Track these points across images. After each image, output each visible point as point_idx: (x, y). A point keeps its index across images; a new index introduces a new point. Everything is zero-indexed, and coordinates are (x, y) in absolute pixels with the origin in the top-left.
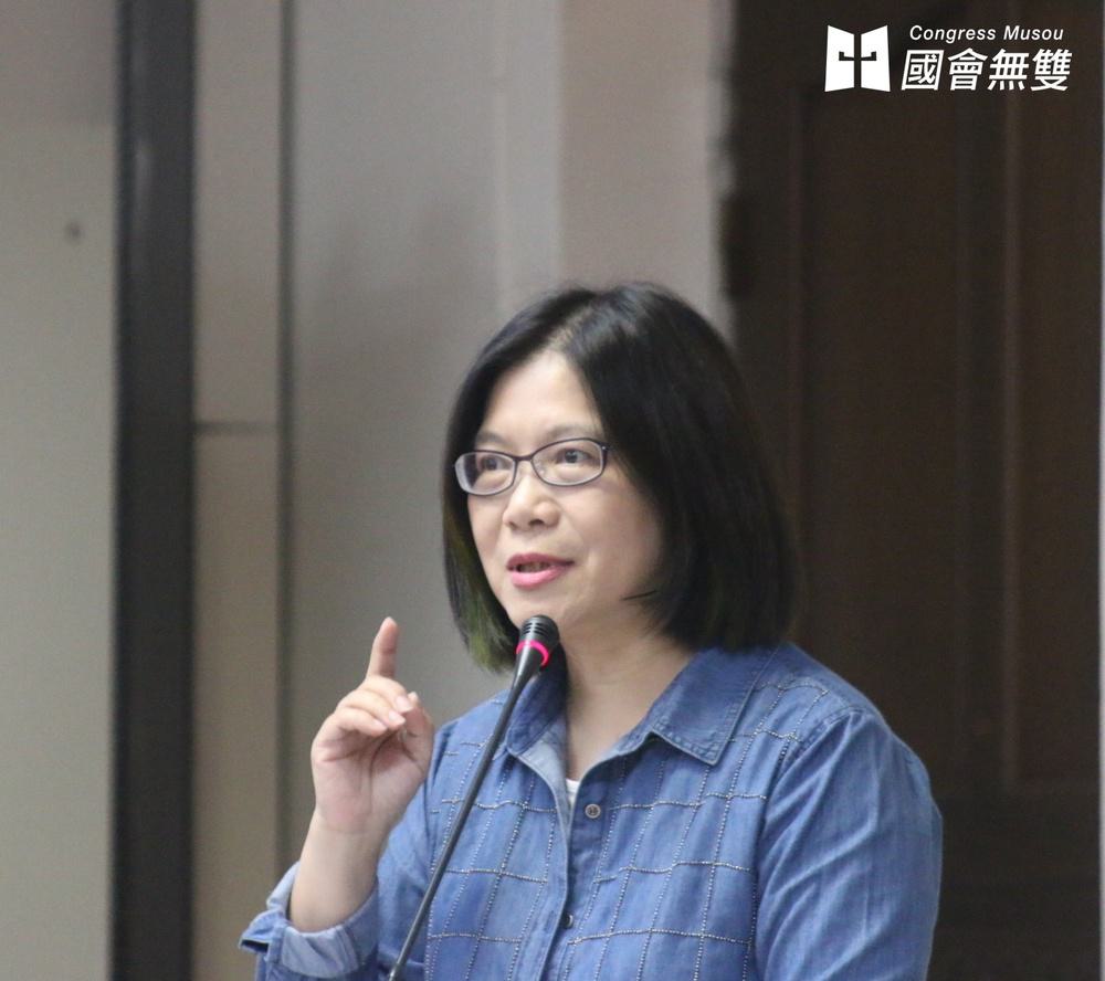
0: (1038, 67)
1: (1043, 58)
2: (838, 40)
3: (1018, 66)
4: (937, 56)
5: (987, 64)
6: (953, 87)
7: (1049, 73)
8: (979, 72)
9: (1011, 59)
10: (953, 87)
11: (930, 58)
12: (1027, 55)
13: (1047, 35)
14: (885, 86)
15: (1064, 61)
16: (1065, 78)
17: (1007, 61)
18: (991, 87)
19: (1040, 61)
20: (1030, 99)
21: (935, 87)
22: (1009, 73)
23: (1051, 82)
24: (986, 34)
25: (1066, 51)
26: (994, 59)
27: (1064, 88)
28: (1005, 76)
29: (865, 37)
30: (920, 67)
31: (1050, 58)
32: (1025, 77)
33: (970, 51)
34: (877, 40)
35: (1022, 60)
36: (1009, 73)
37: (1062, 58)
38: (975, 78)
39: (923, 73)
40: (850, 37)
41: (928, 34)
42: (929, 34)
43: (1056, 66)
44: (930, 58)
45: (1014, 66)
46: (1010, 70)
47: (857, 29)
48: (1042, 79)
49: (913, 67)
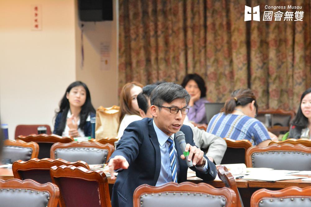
0: (296, 15)
4: (271, 13)
6: (275, 20)
8: (282, 16)
9: (289, 13)
10: (275, 20)
12: (293, 12)
14: (258, 20)
15: (302, 14)
16: (302, 18)
17: (288, 14)
18: (284, 20)
21: (271, 20)
22: (289, 17)
24: (283, 7)
26: (285, 13)
28: (288, 18)
29: (254, 8)
30: (267, 15)
32: (293, 18)
33: (279, 11)
36: (289, 17)
37: (302, 13)
38: (281, 18)
39: (268, 16)
40: (250, 8)
43: (300, 15)
45: (290, 15)
48: (297, 18)
49: (266, 15)
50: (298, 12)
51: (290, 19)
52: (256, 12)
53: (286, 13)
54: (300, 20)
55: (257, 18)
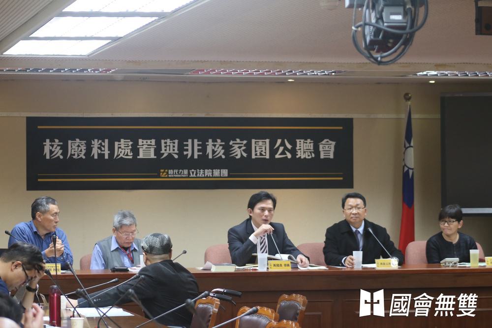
0: (460, 303)
1: (463, 298)
2: (365, 295)
3: (450, 303)
5: (434, 301)
6: (416, 315)
7: (466, 307)
9: (446, 299)
10: (416, 315)
11: (404, 298)
12: (454, 297)
14: (383, 315)
15: (474, 300)
16: (474, 310)
17: (444, 300)
18: (436, 315)
19: (461, 300)
21: (407, 315)
22: (445, 307)
23: (467, 312)
25: (475, 294)
26: (438, 299)
27: (473, 315)
28: (443, 309)
30: (399, 303)
31: (466, 298)
32: (453, 309)
33: (425, 294)
35: (452, 300)
36: (445, 307)
38: (428, 309)
40: (370, 293)
43: (470, 303)
44: (404, 298)
45: (448, 303)
46: (445, 305)
48: (462, 310)
49: (396, 303)
50: (466, 296)
51: (449, 312)
52: (378, 301)
54: (469, 314)
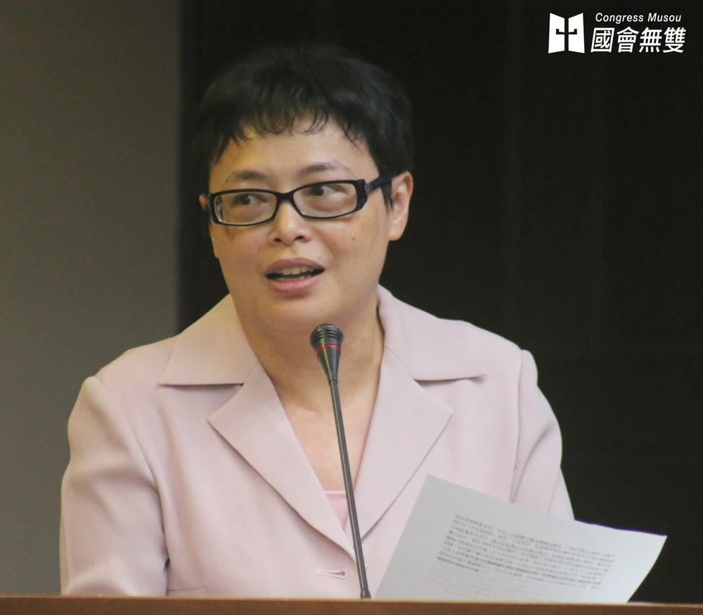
0: (667, 38)
2: (556, 22)
3: (655, 38)
5: (638, 36)
6: (620, 51)
8: (634, 41)
9: (652, 33)
10: (620, 51)
11: (607, 32)
12: (661, 31)
13: (672, 18)
14: (581, 50)
15: (682, 34)
16: (682, 45)
18: (641, 51)
20: (659, 58)
21: (610, 50)
22: (651, 42)
24: (638, 18)
25: (683, 28)
26: (643, 34)
27: (681, 51)
28: (649, 44)
29: (570, 20)
30: (601, 38)
32: (660, 44)
33: (629, 28)
34: (577, 22)
35: (658, 34)
36: (651, 42)
37: (681, 32)
38: (632, 45)
39: (603, 43)
40: (563, 19)
41: (606, 18)
42: (606, 18)
43: (677, 38)
45: (654, 38)
46: (651, 40)
47: (567, 16)
48: (669, 46)
49: (598, 38)
50: (673, 30)
51: (655, 47)
52: (576, 30)
53: (645, 32)
54: (676, 50)
55: (577, 45)
